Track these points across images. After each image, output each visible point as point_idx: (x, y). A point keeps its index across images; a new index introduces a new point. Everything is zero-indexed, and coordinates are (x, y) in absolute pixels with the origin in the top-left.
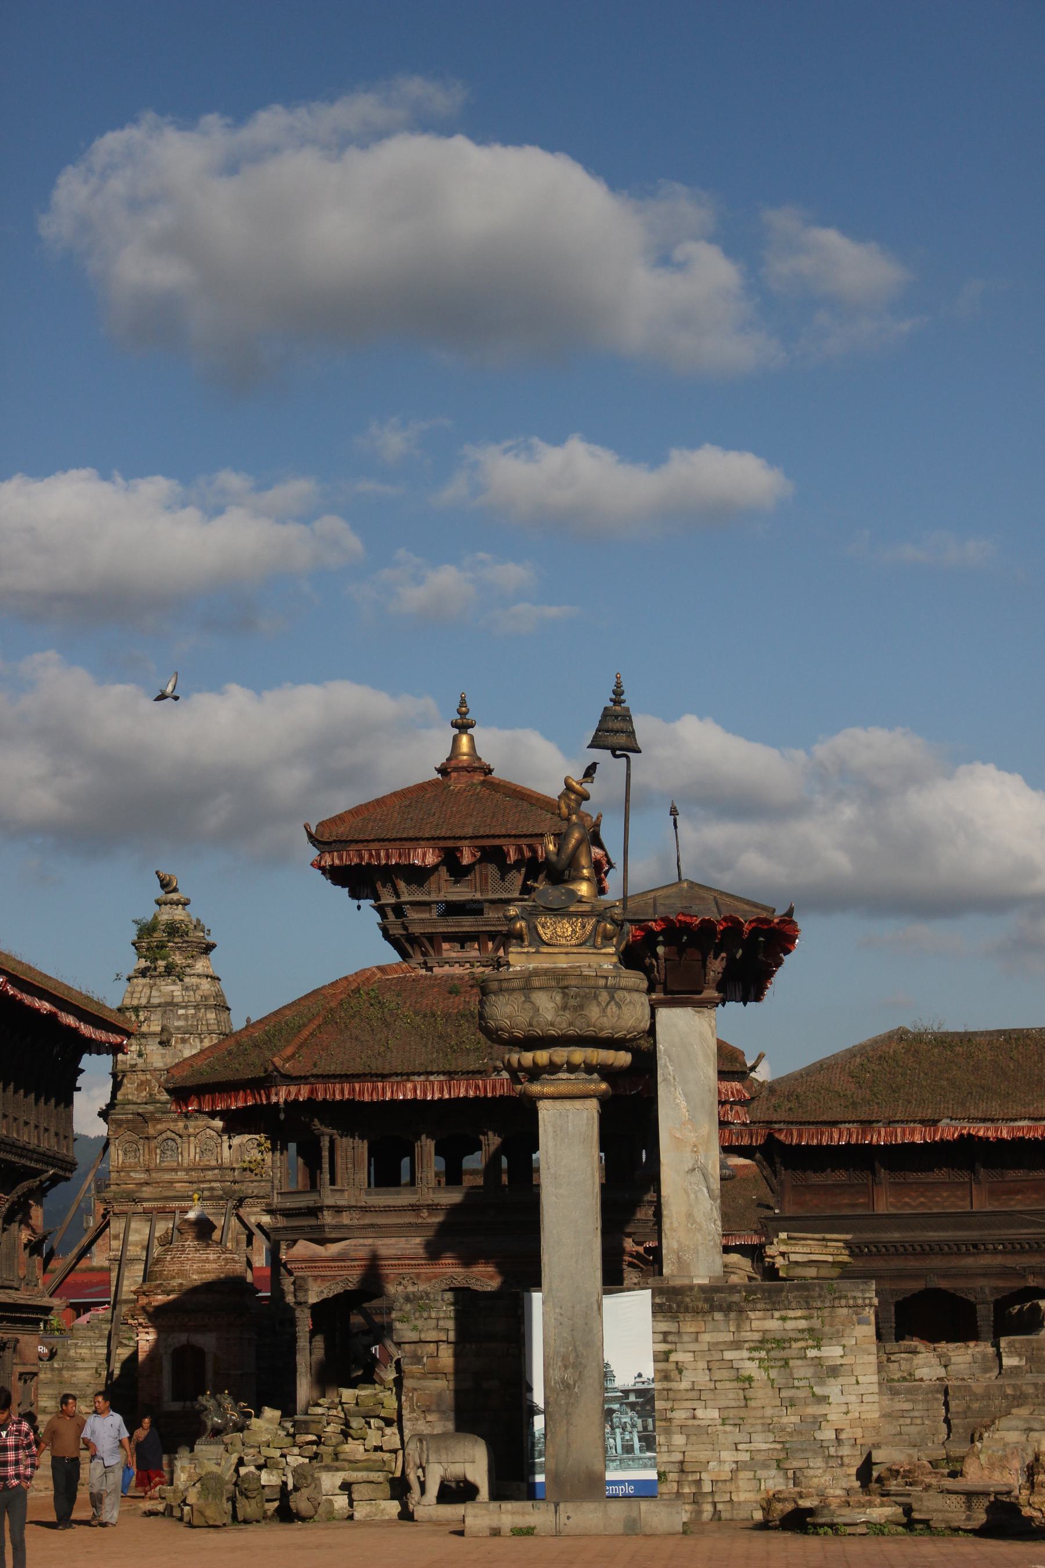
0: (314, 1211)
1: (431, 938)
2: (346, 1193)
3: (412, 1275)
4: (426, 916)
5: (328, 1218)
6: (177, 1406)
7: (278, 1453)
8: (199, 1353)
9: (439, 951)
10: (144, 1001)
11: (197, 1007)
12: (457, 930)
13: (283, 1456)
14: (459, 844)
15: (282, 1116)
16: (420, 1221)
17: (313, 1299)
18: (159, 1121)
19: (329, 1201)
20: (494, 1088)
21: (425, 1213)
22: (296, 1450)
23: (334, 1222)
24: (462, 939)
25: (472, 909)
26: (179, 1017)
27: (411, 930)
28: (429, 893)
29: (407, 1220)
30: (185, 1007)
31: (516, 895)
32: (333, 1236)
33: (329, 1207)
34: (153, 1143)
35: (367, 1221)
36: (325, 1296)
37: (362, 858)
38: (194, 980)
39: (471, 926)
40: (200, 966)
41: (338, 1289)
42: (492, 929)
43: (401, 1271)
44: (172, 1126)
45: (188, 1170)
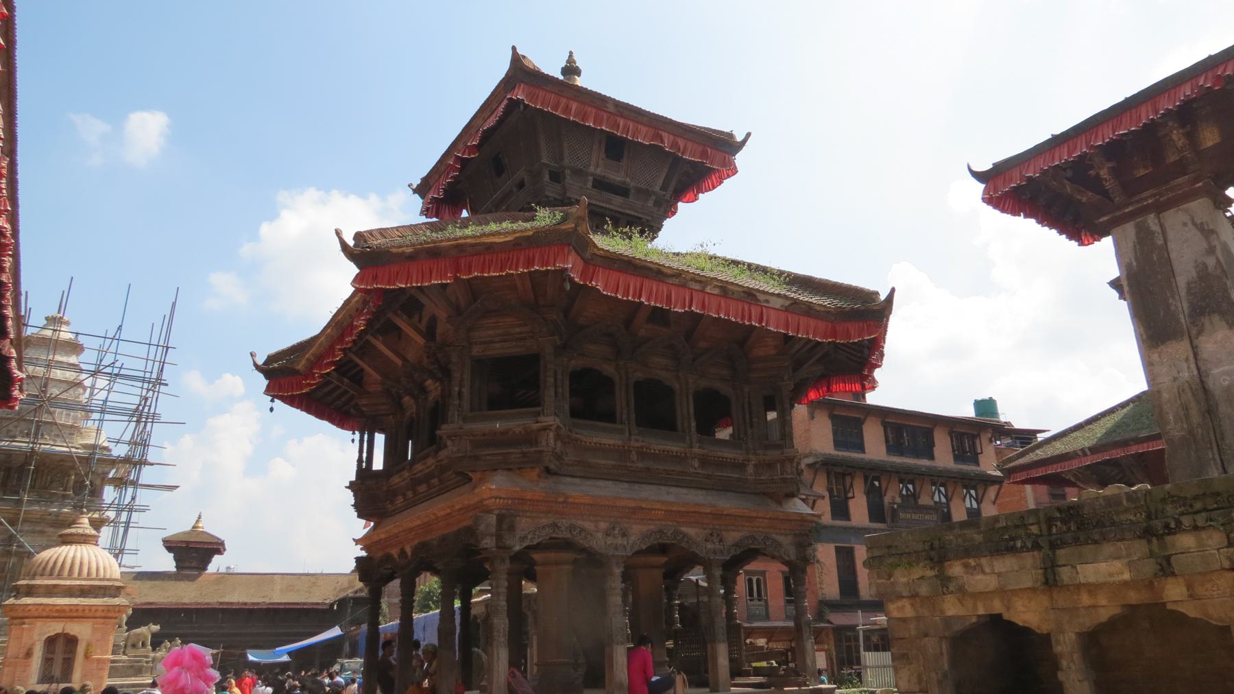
8: (71, 641)
21: (634, 457)
25: (622, 191)
31: (657, 189)
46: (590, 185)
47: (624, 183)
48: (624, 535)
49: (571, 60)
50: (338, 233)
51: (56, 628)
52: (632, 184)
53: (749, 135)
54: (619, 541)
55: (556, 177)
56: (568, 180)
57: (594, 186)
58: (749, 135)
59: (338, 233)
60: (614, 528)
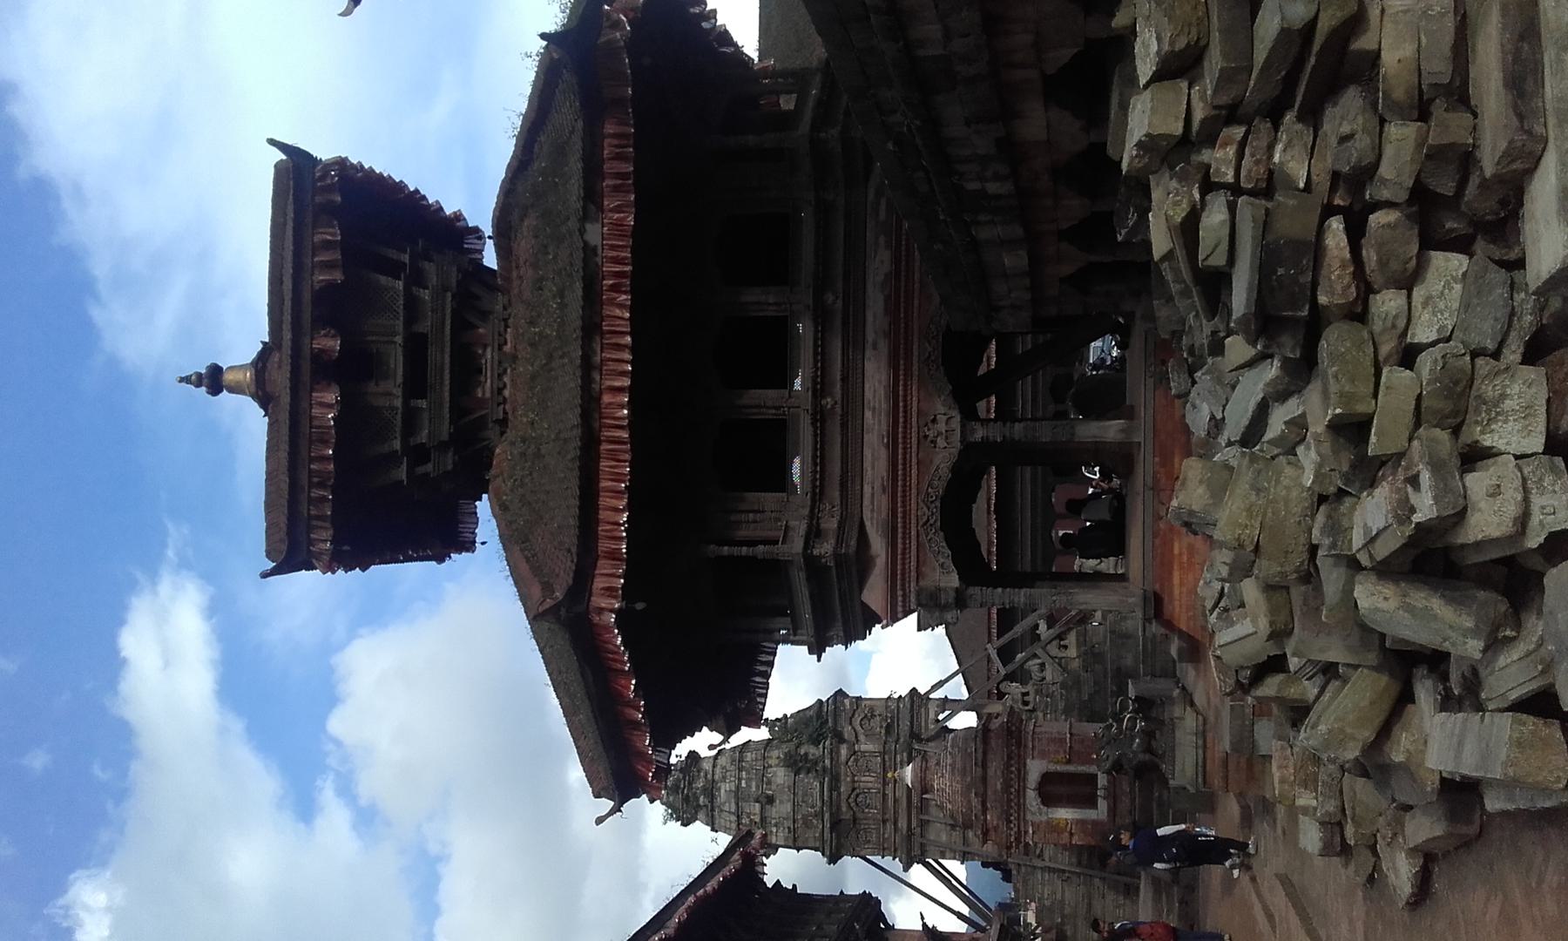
0: (813, 566)
1: (458, 411)
2: (792, 523)
3: (922, 423)
4: (426, 415)
5: (825, 548)
6: (1102, 805)
7: (1396, 376)
8: (1046, 778)
9: (483, 401)
10: (734, 818)
11: (740, 770)
12: (447, 372)
13: (1408, 356)
14: (306, 352)
15: (640, 606)
16: (838, 409)
17: (953, 580)
18: (839, 807)
19: (798, 545)
20: (617, 261)
22: (1387, 303)
23: (833, 541)
24: (467, 369)
25: (416, 348)
26: (749, 786)
27: (445, 437)
28: (393, 408)
29: (838, 429)
30: (740, 780)
32: (853, 543)
33: (807, 545)
34: (859, 815)
35: (835, 494)
36: (949, 563)
37: (323, 499)
38: (718, 770)
39: (443, 352)
40: (707, 766)
41: (940, 538)
42: (448, 322)
43: (914, 440)
44: (844, 797)
45: (885, 784)
46: (423, 404)
47: (405, 347)
48: (934, 421)
49: (198, 380)
50: (600, 821)
51: (1032, 797)
52: (400, 325)
53: (272, 142)
54: (942, 427)
55: (419, 455)
56: (423, 437)
57: (423, 397)
58: (272, 142)
59: (600, 821)
60: (926, 437)
